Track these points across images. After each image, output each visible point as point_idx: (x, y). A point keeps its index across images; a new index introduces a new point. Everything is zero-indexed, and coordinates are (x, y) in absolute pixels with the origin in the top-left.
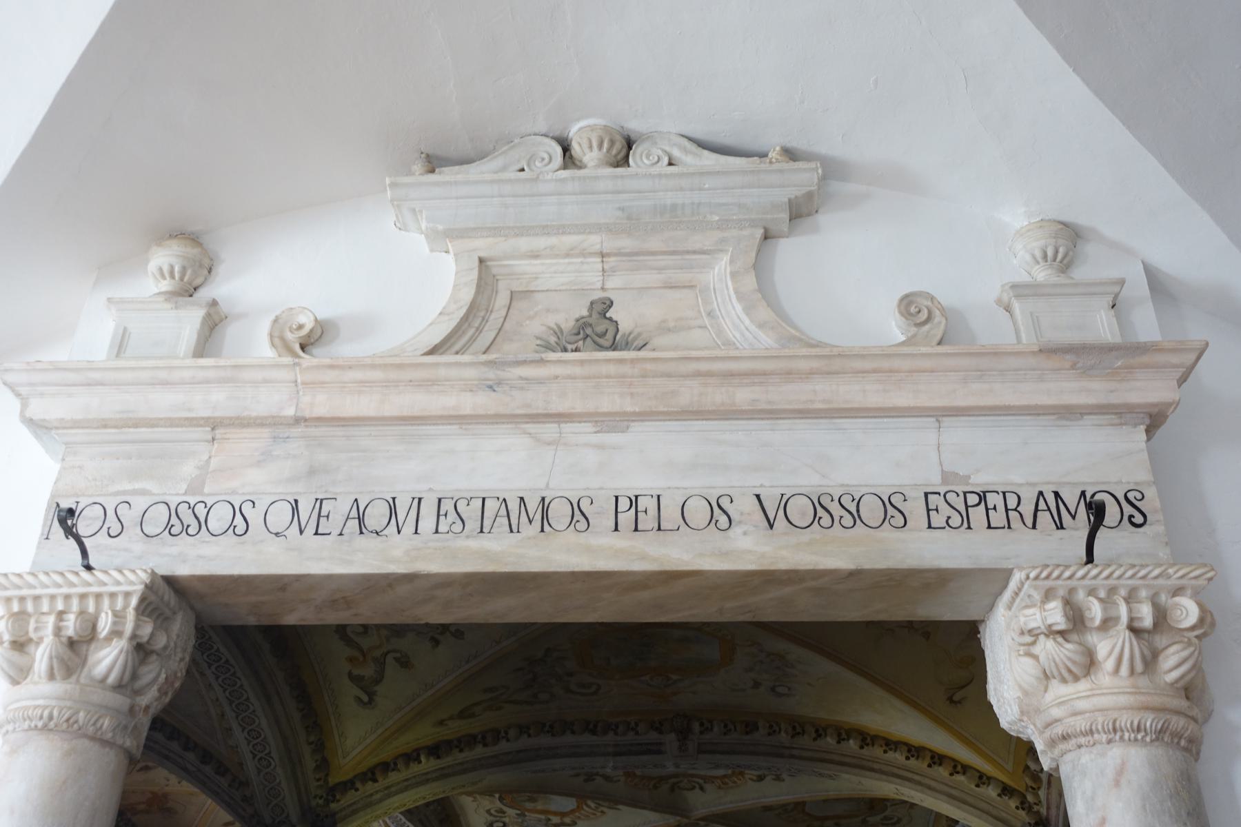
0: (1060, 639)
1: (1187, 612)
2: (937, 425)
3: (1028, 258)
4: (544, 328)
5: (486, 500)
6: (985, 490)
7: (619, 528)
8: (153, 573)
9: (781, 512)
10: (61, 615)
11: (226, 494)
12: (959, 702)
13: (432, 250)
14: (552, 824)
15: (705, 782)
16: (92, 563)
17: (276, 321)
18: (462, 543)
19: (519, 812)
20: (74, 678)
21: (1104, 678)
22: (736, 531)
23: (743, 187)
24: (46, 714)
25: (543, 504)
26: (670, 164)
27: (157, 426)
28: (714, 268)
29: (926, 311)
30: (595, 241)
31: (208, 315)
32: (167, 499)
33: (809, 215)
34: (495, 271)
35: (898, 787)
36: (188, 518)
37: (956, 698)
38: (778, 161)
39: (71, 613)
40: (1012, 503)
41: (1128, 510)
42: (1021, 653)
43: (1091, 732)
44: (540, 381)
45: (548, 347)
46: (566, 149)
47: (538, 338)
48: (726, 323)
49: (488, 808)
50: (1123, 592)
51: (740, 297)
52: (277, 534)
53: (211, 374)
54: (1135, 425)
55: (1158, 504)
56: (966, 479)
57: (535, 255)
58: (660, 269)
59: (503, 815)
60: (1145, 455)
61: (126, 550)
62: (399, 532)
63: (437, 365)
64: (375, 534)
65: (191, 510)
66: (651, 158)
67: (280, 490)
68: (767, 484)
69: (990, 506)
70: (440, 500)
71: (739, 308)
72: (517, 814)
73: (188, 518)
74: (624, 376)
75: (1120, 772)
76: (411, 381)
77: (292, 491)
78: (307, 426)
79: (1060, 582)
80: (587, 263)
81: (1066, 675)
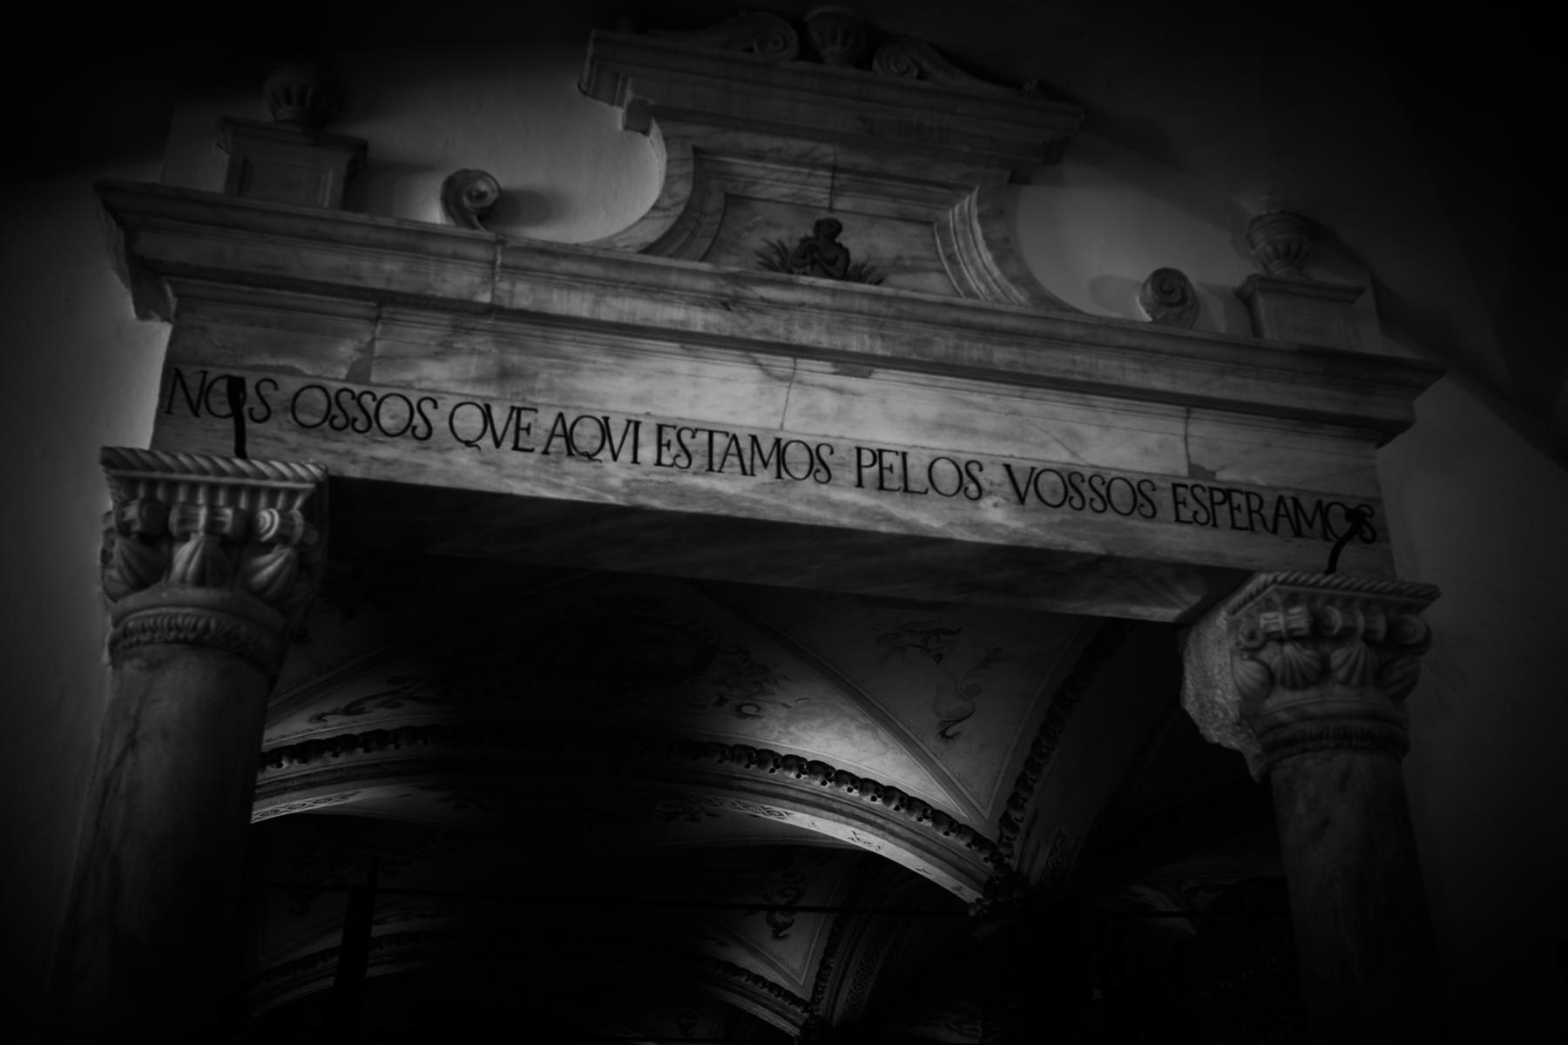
2: (1185, 415)
3: (1269, 250)
4: (764, 244)
5: (717, 438)
7: (864, 483)
8: (326, 471)
9: (1032, 488)
11: (398, 387)
12: (952, 737)
13: (626, 127)
17: (449, 183)
18: (689, 480)
22: (987, 502)
24: (201, 623)
26: (921, 77)
28: (953, 206)
30: (826, 151)
32: (324, 383)
35: (857, 831)
36: (354, 412)
37: (949, 733)
40: (1255, 504)
44: (784, 306)
45: (771, 266)
47: (759, 255)
48: (968, 271)
52: (468, 444)
56: (1211, 475)
57: (758, 156)
61: (277, 439)
63: (669, 269)
64: (586, 458)
65: (354, 402)
66: (899, 65)
67: (467, 390)
68: (1016, 454)
69: (1235, 505)
71: (988, 257)
73: (354, 412)
74: (877, 315)
76: (634, 283)
78: (497, 319)
80: (816, 176)
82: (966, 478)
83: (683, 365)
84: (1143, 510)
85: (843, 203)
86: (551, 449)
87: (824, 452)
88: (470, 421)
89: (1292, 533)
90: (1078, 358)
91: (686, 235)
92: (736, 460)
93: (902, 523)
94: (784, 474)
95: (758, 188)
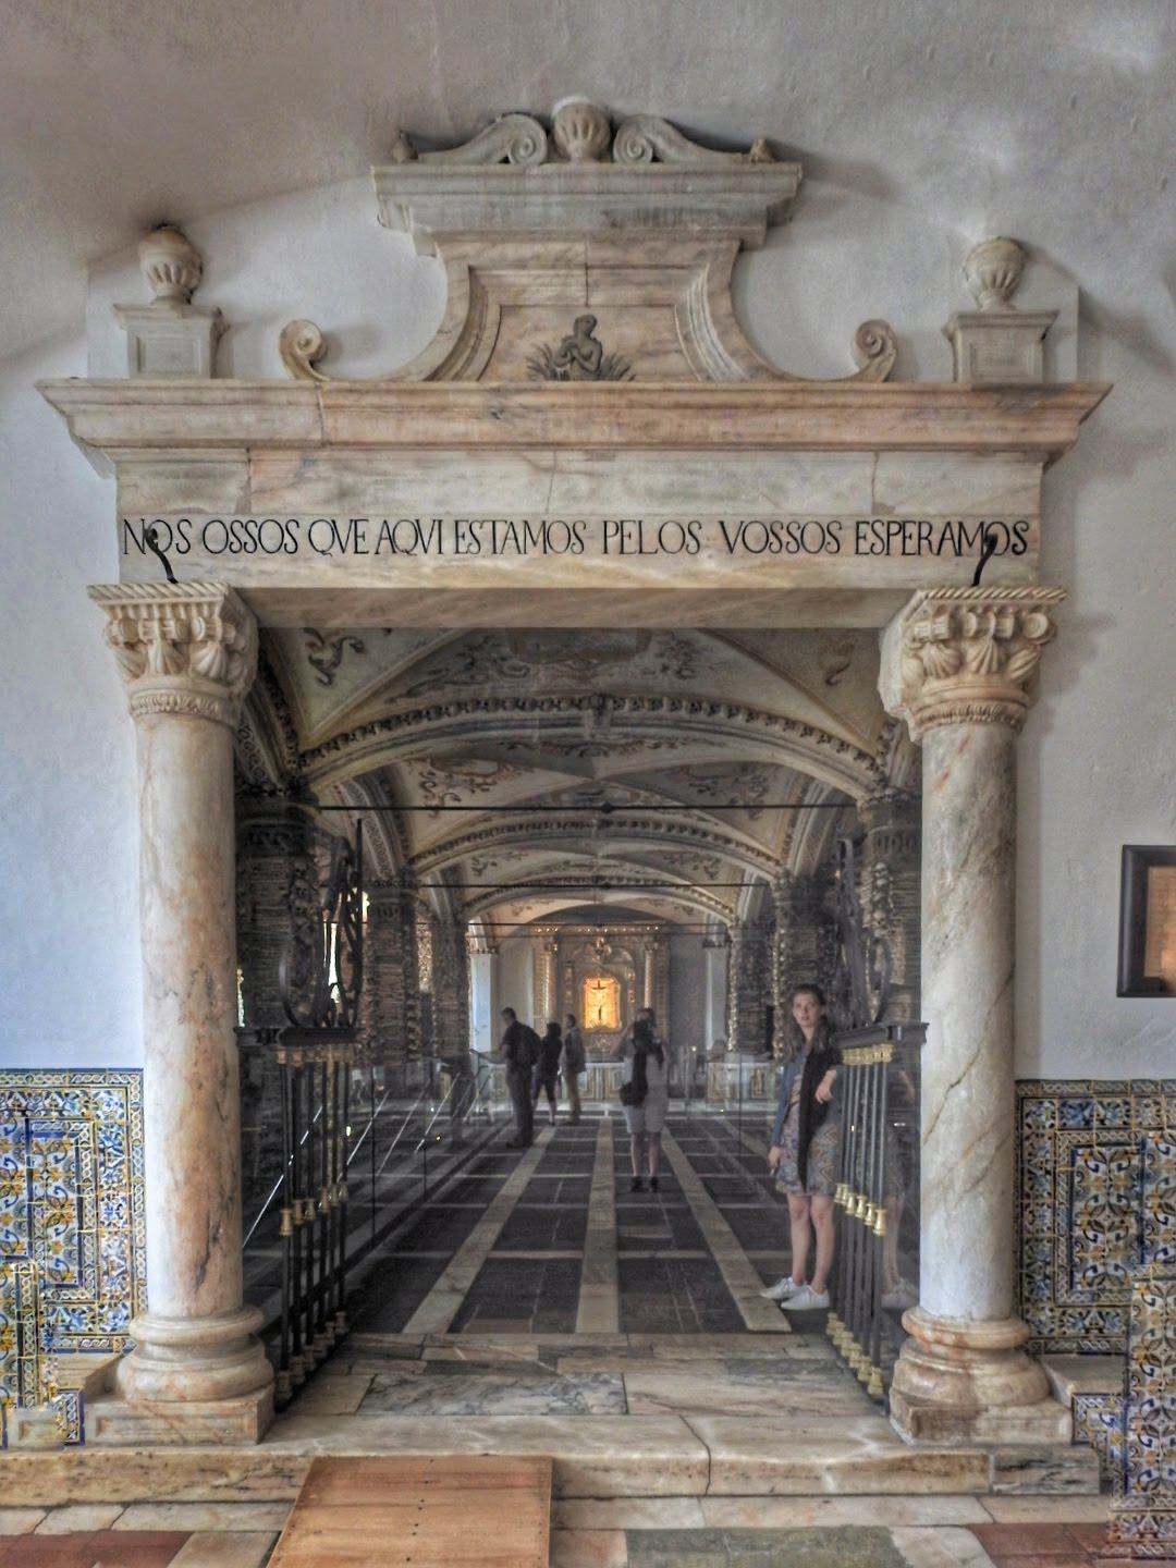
0: (942, 646)
1: (1039, 624)
3: (978, 282)
4: (534, 350)
9: (740, 539)
13: (419, 254)
16: (176, 577)
17: (284, 335)
20: (183, 673)
21: (968, 677)
22: (704, 554)
23: (725, 191)
26: (655, 159)
27: (197, 447)
29: (880, 342)
31: (215, 326)
33: (784, 223)
34: (483, 281)
36: (245, 538)
38: (761, 161)
40: (924, 534)
41: (1014, 539)
43: (950, 715)
44: (538, 410)
46: (549, 130)
47: (529, 359)
50: (995, 609)
51: (716, 321)
52: (323, 552)
53: (238, 395)
54: (1035, 462)
55: (1038, 535)
56: (890, 510)
57: (522, 264)
58: (641, 285)
60: (1037, 491)
69: (907, 534)
70: (457, 523)
71: (714, 333)
73: (245, 538)
74: (612, 407)
75: (965, 742)
76: (423, 407)
77: (332, 511)
81: (941, 673)
83: (469, 468)
84: (829, 548)
85: (597, 298)
87: (579, 528)
88: (322, 535)
90: (781, 421)
91: (469, 350)
93: (636, 579)
95: (526, 296)
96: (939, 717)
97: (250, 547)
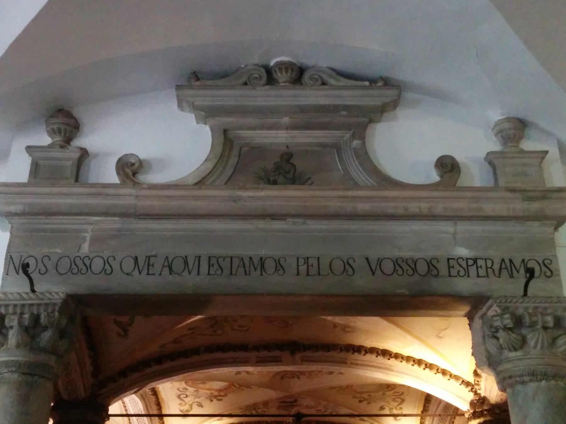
0: (510, 332)
5: (234, 260)
6: (477, 257)
7: (300, 273)
9: (378, 267)
10: (22, 314)
12: (440, 337)
13: (197, 123)
14: (213, 396)
15: (301, 374)
16: (36, 289)
19: (195, 389)
25: (261, 262)
36: (81, 266)
37: (440, 335)
39: (26, 314)
40: (489, 265)
41: (544, 268)
42: (490, 336)
49: (178, 387)
52: (128, 274)
59: (186, 391)
62: (190, 273)
64: (178, 275)
65: (82, 261)
69: (479, 266)
70: (210, 258)
72: (194, 390)
73: (81, 266)
79: (511, 304)
81: (512, 348)
82: (347, 266)
84: (432, 273)
86: (162, 273)
87: (282, 261)
88: (129, 265)
89: (509, 277)
92: (242, 269)
94: (263, 273)
96: (515, 377)
97: (84, 271)
